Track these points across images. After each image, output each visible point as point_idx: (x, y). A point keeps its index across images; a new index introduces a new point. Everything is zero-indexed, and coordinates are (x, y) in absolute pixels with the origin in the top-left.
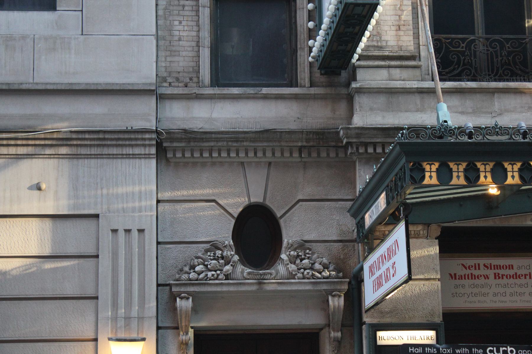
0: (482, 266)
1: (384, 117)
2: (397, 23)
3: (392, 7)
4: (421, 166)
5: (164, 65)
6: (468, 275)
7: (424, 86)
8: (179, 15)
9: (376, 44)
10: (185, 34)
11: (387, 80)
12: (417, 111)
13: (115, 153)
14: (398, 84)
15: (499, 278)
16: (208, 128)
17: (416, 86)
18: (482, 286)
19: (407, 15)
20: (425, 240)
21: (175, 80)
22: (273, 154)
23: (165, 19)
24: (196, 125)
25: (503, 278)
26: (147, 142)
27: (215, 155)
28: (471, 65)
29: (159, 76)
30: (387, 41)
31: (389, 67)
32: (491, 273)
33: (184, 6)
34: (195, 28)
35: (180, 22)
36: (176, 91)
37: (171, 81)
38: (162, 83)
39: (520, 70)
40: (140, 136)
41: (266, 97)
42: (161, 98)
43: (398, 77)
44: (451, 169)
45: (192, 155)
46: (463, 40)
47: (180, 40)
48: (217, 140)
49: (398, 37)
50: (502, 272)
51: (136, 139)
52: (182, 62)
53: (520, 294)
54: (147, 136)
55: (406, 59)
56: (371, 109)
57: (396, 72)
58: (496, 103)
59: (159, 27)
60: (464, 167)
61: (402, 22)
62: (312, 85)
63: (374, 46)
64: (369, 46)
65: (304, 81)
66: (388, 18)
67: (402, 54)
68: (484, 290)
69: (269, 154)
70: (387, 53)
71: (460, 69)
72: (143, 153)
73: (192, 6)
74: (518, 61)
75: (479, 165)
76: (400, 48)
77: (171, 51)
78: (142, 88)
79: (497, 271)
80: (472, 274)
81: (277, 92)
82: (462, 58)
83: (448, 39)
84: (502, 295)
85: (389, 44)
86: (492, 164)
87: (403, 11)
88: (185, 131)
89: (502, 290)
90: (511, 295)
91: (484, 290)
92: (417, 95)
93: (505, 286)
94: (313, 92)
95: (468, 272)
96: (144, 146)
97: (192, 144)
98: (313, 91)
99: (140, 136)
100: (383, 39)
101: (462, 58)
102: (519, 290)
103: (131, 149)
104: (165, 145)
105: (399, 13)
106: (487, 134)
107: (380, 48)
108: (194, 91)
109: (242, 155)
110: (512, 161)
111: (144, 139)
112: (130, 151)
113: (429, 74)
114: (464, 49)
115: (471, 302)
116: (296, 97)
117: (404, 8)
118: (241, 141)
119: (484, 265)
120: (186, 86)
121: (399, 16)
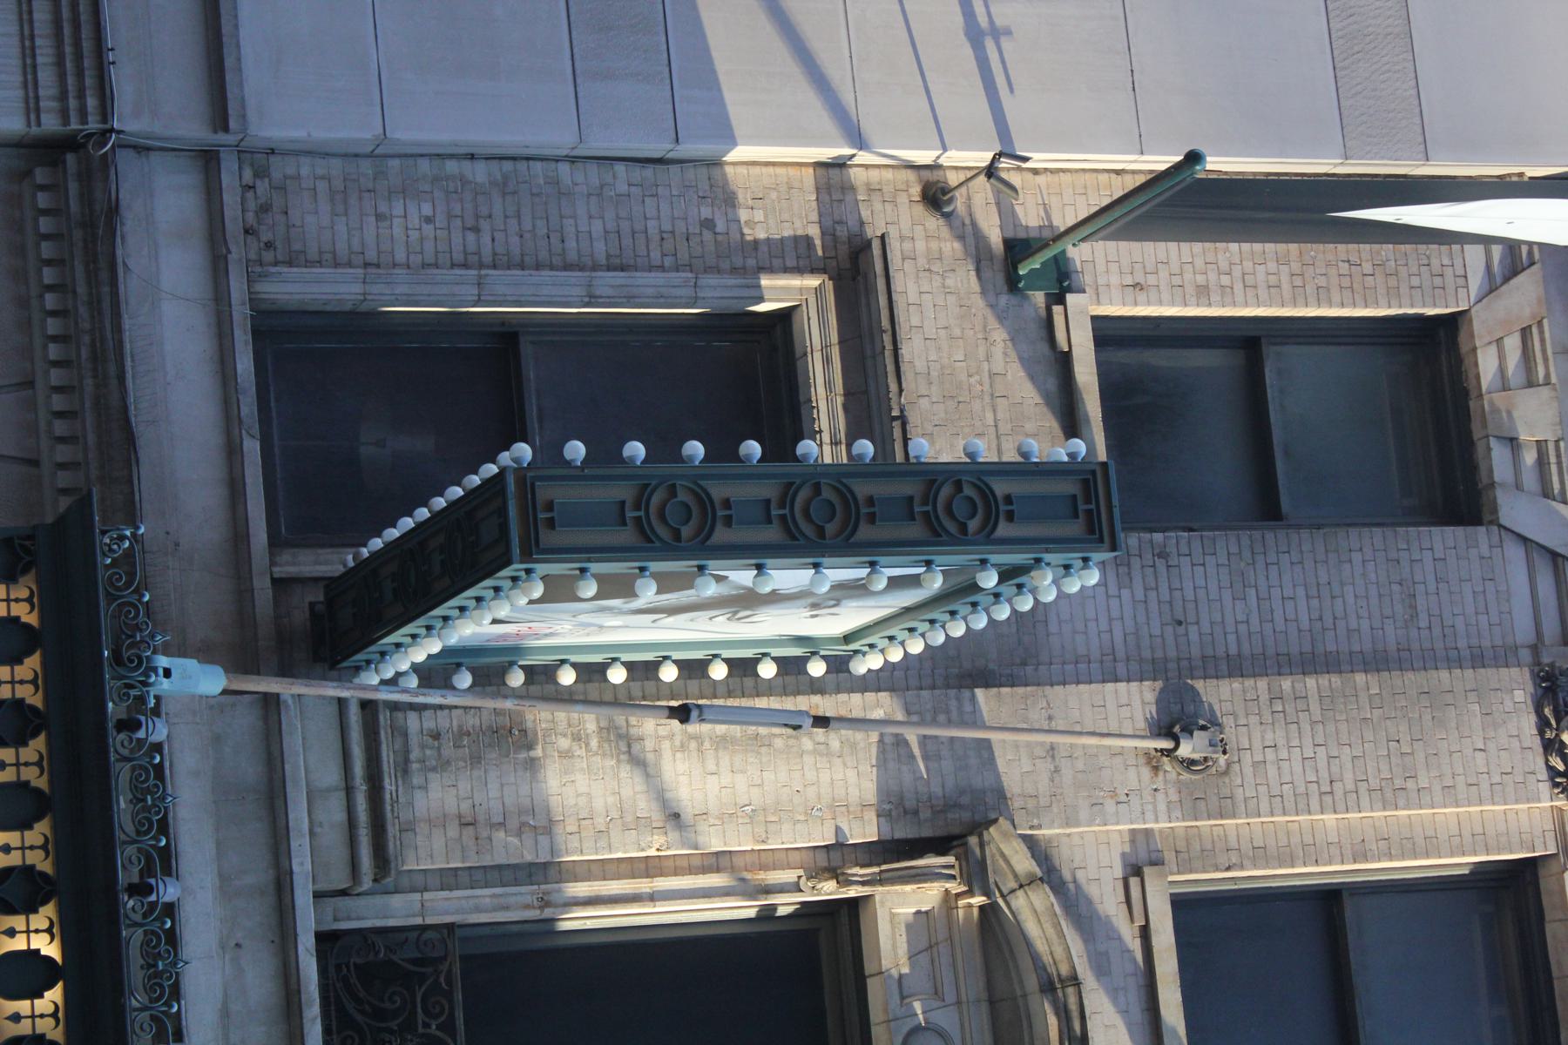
2: (481, 818)
3: (527, 802)
4: (25, 571)
5: (305, 171)
7: (298, 893)
8: (450, 216)
9: (415, 754)
10: (398, 231)
11: (308, 785)
12: (222, 876)
13: (36, 16)
14: (298, 815)
16: (131, 287)
17: (295, 868)
19: (508, 848)
21: (262, 200)
22: (62, 466)
23: (436, 179)
24: (133, 250)
26: (73, 103)
27: (51, 301)
29: (272, 159)
30: (425, 788)
31: (349, 790)
33: (476, 230)
34: (416, 260)
35: (429, 220)
36: (231, 199)
37: (260, 191)
38: (252, 165)
40: (89, 82)
41: (233, 452)
42: (208, 159)
44: (20, 662)
45: (46, 237)
47: (379, 217)
48: (94, 304)
51: (80, 74)
52: (314, 220)
54: (92, 102)
56: (217, 740)
57: (333, 811)
59: (411, 161)
60: (29, 701)
61: (484, 834)
62: (277, 583)
63: (407, 751)
64: (406, 735)
65: (287, 564)
66: (494, 792)
67: (392, 830)
69: (63, 453)
70: (389, 785)
71: (359, 1018)
72: (41, 92)
73: (478, 253)
75: (38, 744)
76: (409, 828)
77: (345, 192)
78: (229, 95)
81: (248, 480)
82: (394, 1025)
83: (449, 981)
85: (418, 794)
86: (42, 783)
88: (114, 210)
92: (271, 874)
94: (257, 583)
96: (63, 96)
97: (78, 234)
98: (262, 587)
99: (89, 82)
100: (431, 776)
101: (394, 1025)
103: (50, 60)
104: (70, 158)
105: (513, 823)
106: (133, 769)
107: (404, 768)
108: (233, 248)
109: (56, 376)
110: (50, 764)
111: (81, 96)
112: (45, 57)
113: (336, 919)
114: (421, 1030)
116: (239, 536)
117: (528, 838)
118: (95, 370)
120: (247, 232)
121: (502, 824)
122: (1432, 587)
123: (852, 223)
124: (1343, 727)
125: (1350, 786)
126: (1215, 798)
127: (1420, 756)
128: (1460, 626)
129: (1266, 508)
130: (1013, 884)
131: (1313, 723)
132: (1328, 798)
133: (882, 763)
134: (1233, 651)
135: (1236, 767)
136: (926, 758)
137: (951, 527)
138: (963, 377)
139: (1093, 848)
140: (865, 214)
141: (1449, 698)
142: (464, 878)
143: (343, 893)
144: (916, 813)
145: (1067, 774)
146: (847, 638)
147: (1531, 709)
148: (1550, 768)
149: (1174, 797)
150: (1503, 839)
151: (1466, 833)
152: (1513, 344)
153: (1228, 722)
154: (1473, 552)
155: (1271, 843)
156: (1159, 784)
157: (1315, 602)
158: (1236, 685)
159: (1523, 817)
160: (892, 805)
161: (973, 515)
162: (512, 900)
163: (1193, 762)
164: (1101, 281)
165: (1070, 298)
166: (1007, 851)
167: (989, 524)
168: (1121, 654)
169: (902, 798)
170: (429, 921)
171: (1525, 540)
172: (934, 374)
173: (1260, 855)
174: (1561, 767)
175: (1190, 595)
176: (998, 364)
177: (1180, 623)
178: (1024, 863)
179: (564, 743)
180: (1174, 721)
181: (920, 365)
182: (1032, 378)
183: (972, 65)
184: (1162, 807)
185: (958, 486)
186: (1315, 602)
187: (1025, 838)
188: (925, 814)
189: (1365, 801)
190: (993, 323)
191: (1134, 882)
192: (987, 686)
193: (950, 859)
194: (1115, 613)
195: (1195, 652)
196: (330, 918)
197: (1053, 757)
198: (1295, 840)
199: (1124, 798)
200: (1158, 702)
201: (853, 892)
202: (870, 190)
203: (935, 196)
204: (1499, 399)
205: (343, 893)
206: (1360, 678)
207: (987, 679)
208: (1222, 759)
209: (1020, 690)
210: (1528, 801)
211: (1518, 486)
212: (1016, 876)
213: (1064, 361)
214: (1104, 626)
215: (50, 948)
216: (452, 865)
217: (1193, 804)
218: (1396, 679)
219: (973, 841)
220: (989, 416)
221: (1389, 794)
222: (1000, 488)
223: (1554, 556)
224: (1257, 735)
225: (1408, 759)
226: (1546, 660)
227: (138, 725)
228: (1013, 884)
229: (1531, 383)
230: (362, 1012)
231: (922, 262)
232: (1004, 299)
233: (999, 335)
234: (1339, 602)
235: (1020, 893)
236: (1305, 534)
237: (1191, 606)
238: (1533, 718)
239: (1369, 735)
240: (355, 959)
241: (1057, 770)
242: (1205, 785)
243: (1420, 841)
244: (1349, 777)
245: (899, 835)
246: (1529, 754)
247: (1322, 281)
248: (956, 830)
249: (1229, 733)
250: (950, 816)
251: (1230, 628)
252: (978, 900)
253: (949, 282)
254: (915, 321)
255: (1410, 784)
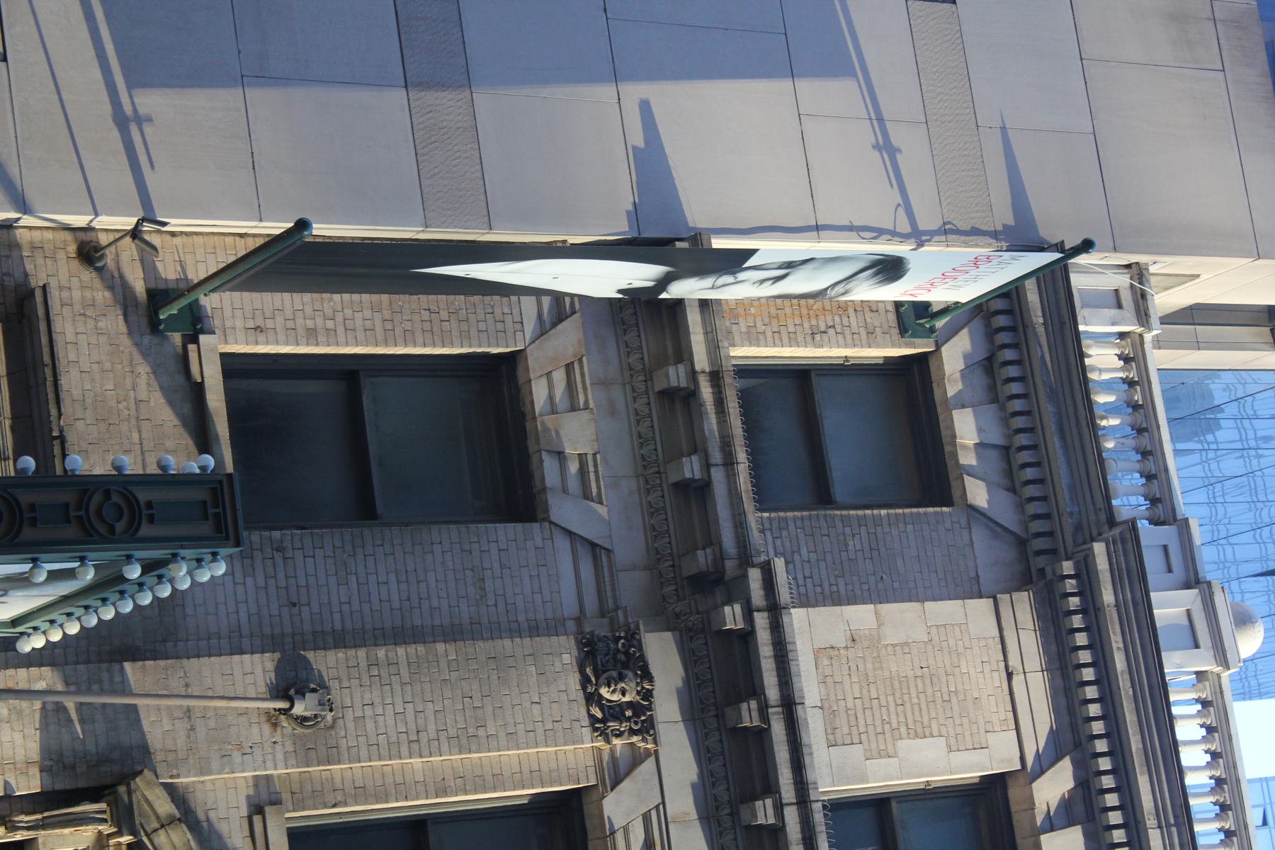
122: (497, 573)
123: (18, 275)
124: (427, 687)
125: (433, 735)
126: (323, 749)
127: (489, 709)
128: (520, 603)
129: (364, 509)
130: (156, 825)
131: (403, 684)
132: (416, 745)
133: (44, 727)
134: (338, 626)
135: (341, 722)
136: (82, 721)
137: (102, 529)
138: (113, 403)
139: (223, 792)
140: (29, 267)
141: (511, 662)
144: (73, 767)
145: (201, 732)
146: (15, 622)
147: (576, 669)
148: (591, 716)
149: (290, 748)
150: (554, 775)
151: (526, 770)
152: (559, 377)
153: (334, 685)
154: (530, 544)
155: (369, 783)
156: (278, 738)
157: (404, 586)
158: (341, 655)
159: (571, 756)
160: (53, 761)
161: (119, 519)
163: (305, 719)
164: (228, 324)
165: (203, 338)
166: (150, 798)
167: (134, 526)
168: (246, 631)
169: (61, 755)
171: (570, 533)
172: (88, 401)
173: (361, 793)
174: (599, 715)
175: (302, 582)
176: (143, 395)
177: (294, 605)
178: (165, 807)
180: (291, 684)
181: (76, 393)
182: (171, 403)
183: (119, 146)
184: (280, 756)
185: (107, 494)
186: (404, 586)
187: (165, 785)
188: (81, 768)
189: (445, 747)
190: (138, 358)
191: (257, 819)
192: (134, 660)
193: (103, 806)
194: (241, 597)
195: (307, 628)
197: (189, 717)
198: (389, 780)
199: (248, 750)
200: (277, 670)
201: (19, 836)
202: (33, 247)
203: (89, 252)
204: (549, 420)
206: (440, 647)
207: (135, 655)
208: (329, 716)
209: (162, 663)
210: (574, 743)
211: (565, 490)
212: (158, 817)
213: (198, 390)
214: (232, 608)
217: (305, 753)
218: (469, 647)
219: (122, 789)
220: (135, 436)
221: (464, 741)
222: (143, 496)
223: (593, 546)
224: (357, 696)
225: (479, 712)
226: (587, 629)
228: (156, 825)
229: (573, 408)
231: (78, 308)
232: (147, 340)
233: (143, 369)
234: (423, 585)
235: (162, 832)
236: (396, 530)
237: (303, 591)
238: (577, 676)
239: (448, 694)
241: (192, 729)
242: (316, 739)
243: (489, 778)
244: (432, 727)
245: (58, 787)
246: (575, 705)
247: (408, 326)
248: (107, 782)
249: (335, 694)
250: (103, 769)
251: (336, 608)
252: (126, 839)
253: (101, 324)
254: (72, 357)
255: (481, 732)
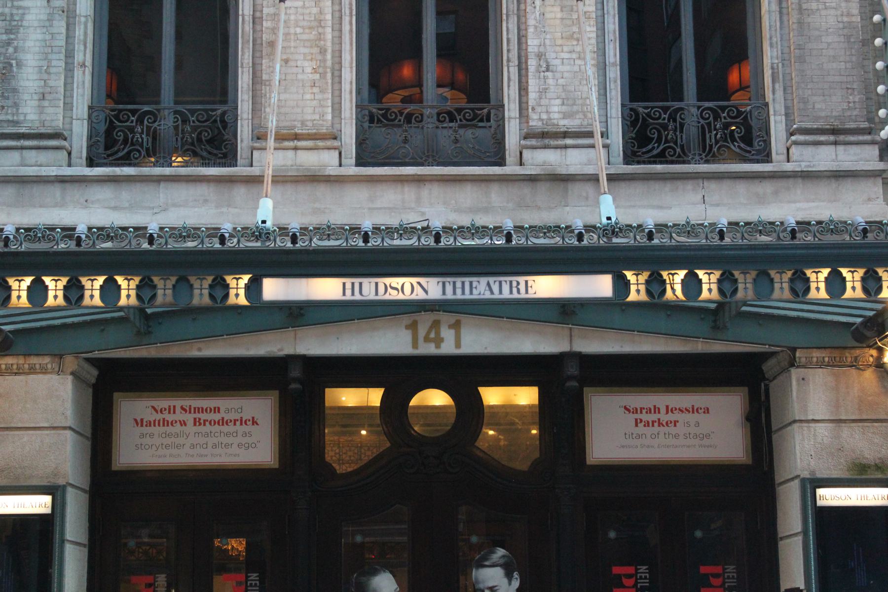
0: (178, 409)
1: (9, 214)
2: (41, 91)
3: (36, 69)
6: (159, 421)
9: (10, 118)
12: (56, 205)
15: (200, 424)
17: (54, 174)
18: (177, 435)
20: (55, 377)
25: (205, 425)
28: (142, 145)
30: (25, 115)
31: (23, 148)
32: (189, 418)
39: (206, 150)
43: (33, 161)
46: (134, 112)
49: (41, 109)
50: (203, 416)
53: (227, 446)
55: (48, 138)
57: (31, 156)
58: (161, 195)
61: (49, 89)
63: (8, 121)
66: (31, 84)
67: (43, 130)
68: (181, 441)
71: (126, 151)
74: (203, 138)
76: (43, 123)
79: (197, 415)
80: (164, 419)
84: (201, 446)
85: (28, 117)
87: (49, 73)
89: (201, 440)
90: (215, 446)
91: (181, 441)
92: (57, 185)
93: (207, 435)
95: (159, 416)
100: (20, 111)
101: (130, 136)
102: (225, 440)
105: (45, 76)
107: (16, 123)
115: (160, 457)
117: (52, 70)
119: (182, 408)
142: (68, 100)
143: (70, 154)
162: (81, 79)
170: (86, 116)
179: (11, 50)
196: (80, 161)
205: (70, 154)
215: (28, 280)
216: (62, 105)
227: (79, 237)
230: (123, 149)
240: (101, 150)
